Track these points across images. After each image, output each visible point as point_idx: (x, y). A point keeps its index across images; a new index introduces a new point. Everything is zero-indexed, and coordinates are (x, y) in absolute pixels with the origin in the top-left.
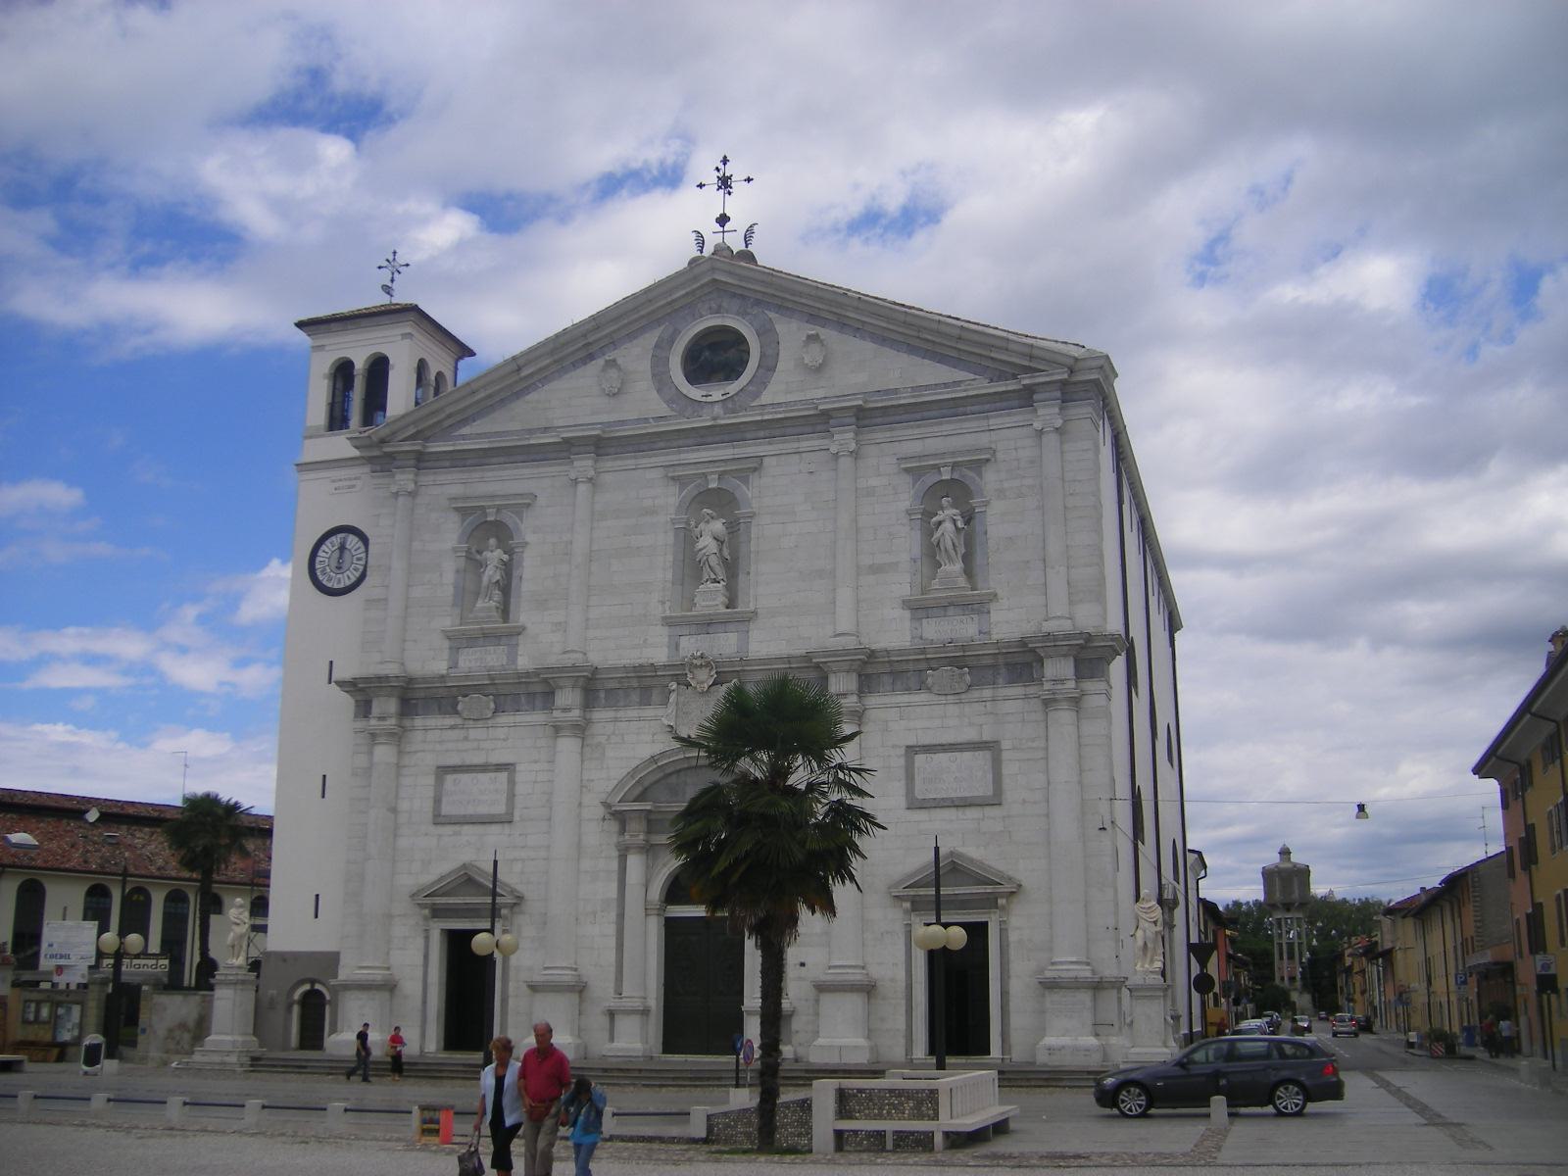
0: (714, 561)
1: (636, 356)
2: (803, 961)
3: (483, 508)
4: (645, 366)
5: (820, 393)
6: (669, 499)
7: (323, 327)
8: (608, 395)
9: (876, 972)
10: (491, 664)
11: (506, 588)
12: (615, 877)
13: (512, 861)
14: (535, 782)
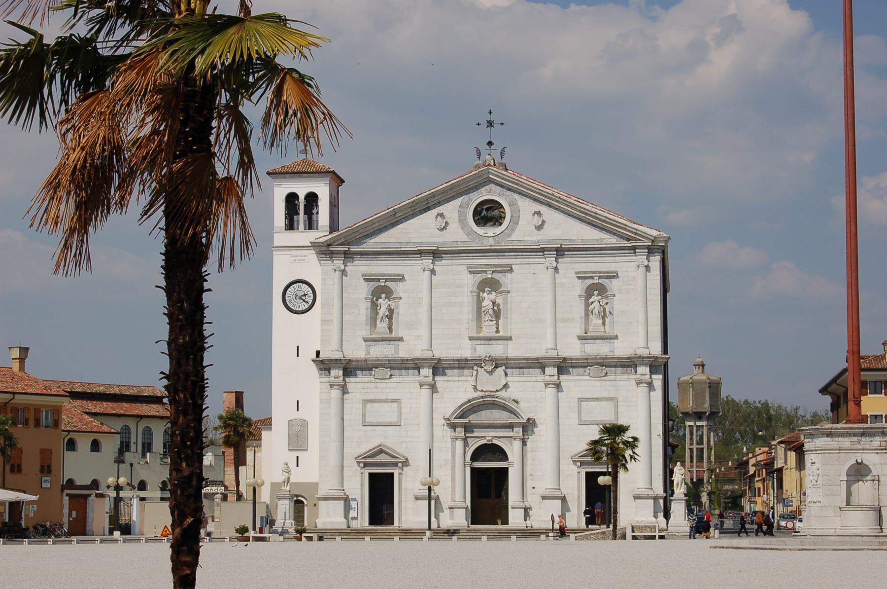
0: (491, 312)
1: (451, 209)
2: (534, 486)
3: (379, 280)
4: (455, 216)
5: (539, 238)
6: (470, 282)
7: (282, 175)
8: (438, 229)
9: (564, 491)
10: (386, 353)
11: (390, 317)
12: (450, 450)
13: (401, 442)
14: (411, 408)
